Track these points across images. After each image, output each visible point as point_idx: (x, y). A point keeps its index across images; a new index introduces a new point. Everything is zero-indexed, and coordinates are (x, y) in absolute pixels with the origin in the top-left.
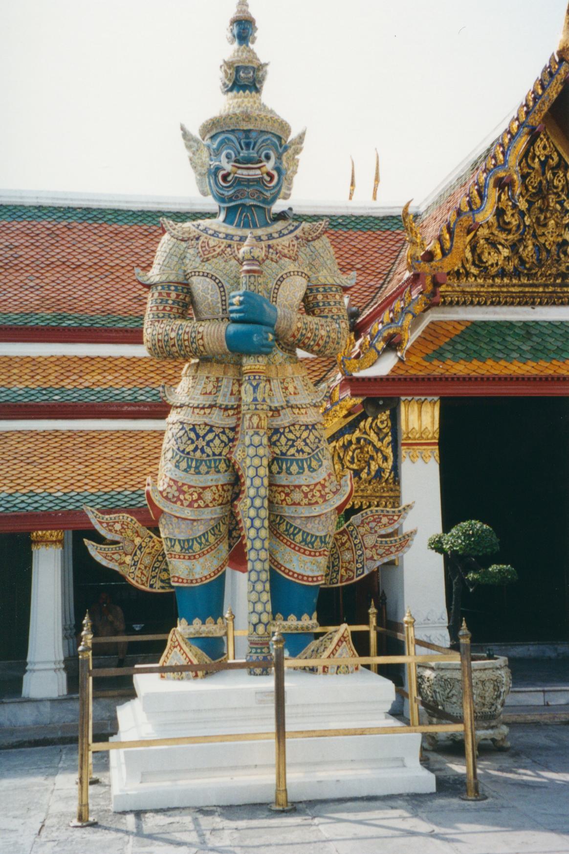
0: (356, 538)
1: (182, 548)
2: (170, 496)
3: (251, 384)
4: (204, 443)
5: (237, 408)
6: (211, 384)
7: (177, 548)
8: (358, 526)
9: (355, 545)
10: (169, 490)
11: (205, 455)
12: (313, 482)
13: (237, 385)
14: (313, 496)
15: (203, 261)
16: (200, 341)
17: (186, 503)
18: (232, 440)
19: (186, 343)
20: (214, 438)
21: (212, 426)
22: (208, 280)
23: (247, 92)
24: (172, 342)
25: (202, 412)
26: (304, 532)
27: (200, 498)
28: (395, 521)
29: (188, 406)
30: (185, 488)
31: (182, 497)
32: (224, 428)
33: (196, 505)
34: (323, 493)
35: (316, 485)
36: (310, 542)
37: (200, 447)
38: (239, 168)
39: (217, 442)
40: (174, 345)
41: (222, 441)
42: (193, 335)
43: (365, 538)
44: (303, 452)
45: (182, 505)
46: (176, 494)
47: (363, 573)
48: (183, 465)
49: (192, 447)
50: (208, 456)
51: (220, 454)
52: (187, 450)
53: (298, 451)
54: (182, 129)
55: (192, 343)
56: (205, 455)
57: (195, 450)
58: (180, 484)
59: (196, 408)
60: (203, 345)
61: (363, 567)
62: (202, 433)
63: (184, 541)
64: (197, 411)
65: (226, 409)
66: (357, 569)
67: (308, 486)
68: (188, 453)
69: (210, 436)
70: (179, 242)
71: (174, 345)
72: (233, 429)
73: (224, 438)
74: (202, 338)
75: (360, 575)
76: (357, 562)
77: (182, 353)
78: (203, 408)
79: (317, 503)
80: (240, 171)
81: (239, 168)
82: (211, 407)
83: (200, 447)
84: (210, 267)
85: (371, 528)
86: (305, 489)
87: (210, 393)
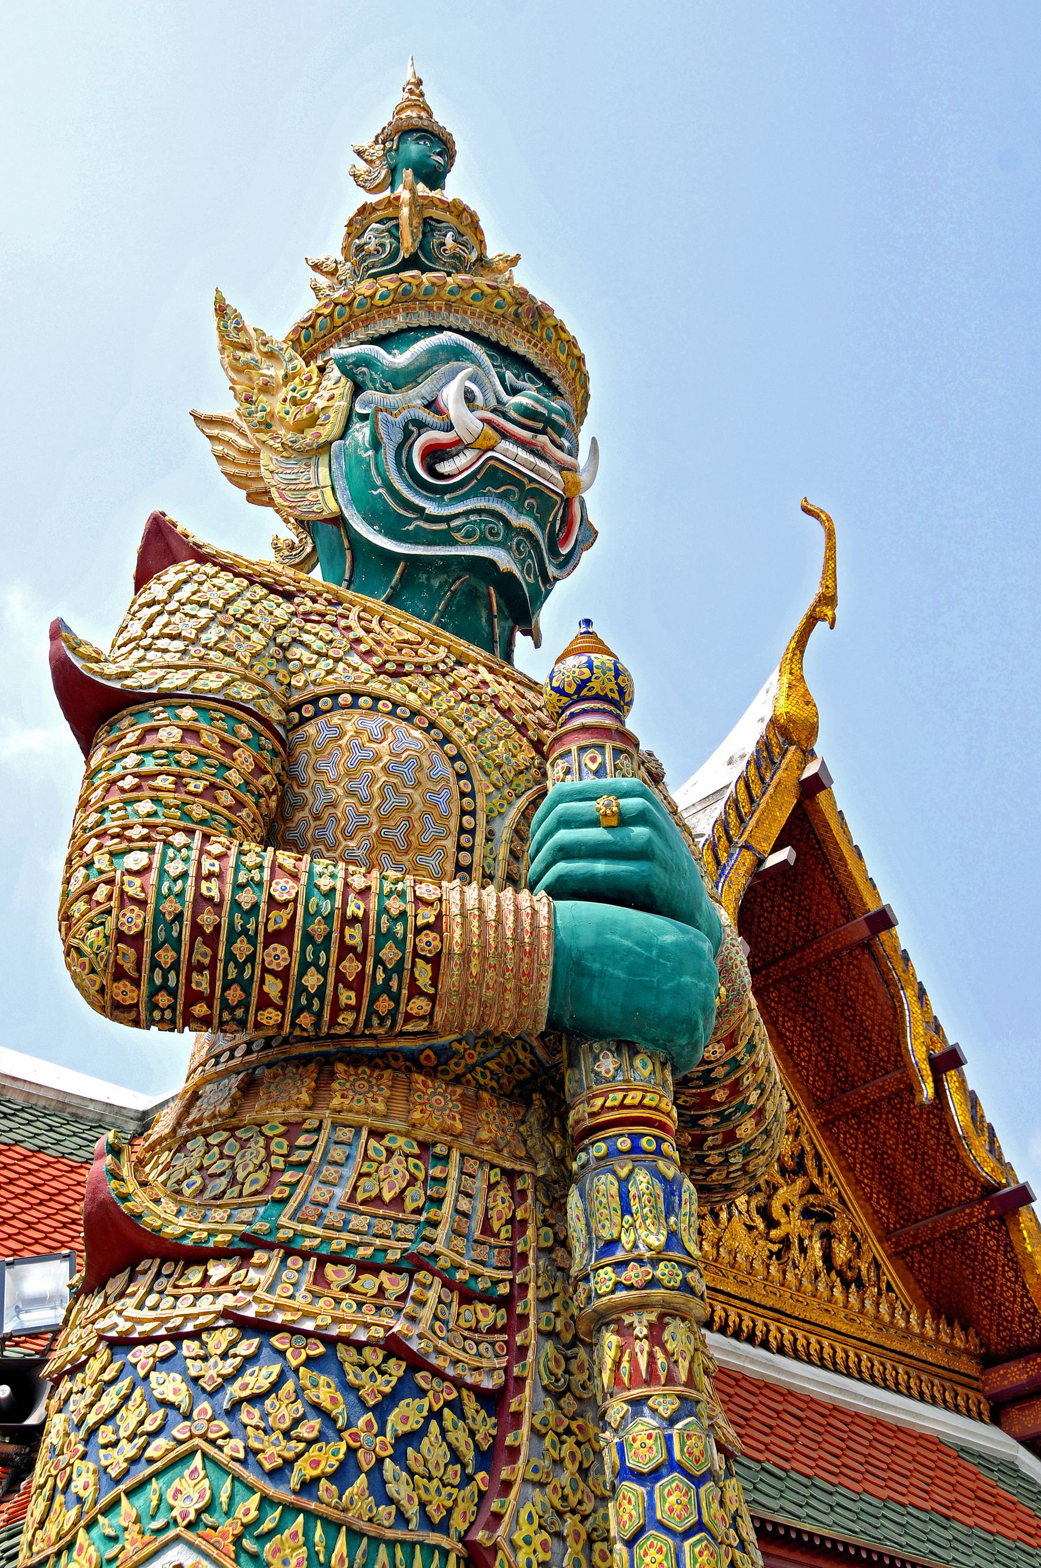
3: (656, 1173)
13: (502, 1192)
19: (354, 935)
20: (427, 1420)
21: (416, 1363)
24: (280, 919)
25: (368, 1283)
29: (289, 1250)
32: (458, 1383)
37: (366, 1460)
38: (505, 435)
39: (432, 1449)
40: (283, 936)
42: (395, 905)
49: (329, 1457)
50: (402, 1519)
52: (303, 1470)
54: (221, 310)
55: (383, 938)
57: (341, 1476)
59: (337, 1259)
62: (375, 1387)
64: (338, 1275)
65: (467, 1297)
68: (309, 1486)
69: (407, 1415)
71: (283, 936)
72: (493, 1401)
73: (460, 1437)
74: (436, 926)
77: (312, 980)
78: (366, 1267)
81: (505, 435)
82: (413, 1264)
83: (366, 1460)
87: (399, 1199)
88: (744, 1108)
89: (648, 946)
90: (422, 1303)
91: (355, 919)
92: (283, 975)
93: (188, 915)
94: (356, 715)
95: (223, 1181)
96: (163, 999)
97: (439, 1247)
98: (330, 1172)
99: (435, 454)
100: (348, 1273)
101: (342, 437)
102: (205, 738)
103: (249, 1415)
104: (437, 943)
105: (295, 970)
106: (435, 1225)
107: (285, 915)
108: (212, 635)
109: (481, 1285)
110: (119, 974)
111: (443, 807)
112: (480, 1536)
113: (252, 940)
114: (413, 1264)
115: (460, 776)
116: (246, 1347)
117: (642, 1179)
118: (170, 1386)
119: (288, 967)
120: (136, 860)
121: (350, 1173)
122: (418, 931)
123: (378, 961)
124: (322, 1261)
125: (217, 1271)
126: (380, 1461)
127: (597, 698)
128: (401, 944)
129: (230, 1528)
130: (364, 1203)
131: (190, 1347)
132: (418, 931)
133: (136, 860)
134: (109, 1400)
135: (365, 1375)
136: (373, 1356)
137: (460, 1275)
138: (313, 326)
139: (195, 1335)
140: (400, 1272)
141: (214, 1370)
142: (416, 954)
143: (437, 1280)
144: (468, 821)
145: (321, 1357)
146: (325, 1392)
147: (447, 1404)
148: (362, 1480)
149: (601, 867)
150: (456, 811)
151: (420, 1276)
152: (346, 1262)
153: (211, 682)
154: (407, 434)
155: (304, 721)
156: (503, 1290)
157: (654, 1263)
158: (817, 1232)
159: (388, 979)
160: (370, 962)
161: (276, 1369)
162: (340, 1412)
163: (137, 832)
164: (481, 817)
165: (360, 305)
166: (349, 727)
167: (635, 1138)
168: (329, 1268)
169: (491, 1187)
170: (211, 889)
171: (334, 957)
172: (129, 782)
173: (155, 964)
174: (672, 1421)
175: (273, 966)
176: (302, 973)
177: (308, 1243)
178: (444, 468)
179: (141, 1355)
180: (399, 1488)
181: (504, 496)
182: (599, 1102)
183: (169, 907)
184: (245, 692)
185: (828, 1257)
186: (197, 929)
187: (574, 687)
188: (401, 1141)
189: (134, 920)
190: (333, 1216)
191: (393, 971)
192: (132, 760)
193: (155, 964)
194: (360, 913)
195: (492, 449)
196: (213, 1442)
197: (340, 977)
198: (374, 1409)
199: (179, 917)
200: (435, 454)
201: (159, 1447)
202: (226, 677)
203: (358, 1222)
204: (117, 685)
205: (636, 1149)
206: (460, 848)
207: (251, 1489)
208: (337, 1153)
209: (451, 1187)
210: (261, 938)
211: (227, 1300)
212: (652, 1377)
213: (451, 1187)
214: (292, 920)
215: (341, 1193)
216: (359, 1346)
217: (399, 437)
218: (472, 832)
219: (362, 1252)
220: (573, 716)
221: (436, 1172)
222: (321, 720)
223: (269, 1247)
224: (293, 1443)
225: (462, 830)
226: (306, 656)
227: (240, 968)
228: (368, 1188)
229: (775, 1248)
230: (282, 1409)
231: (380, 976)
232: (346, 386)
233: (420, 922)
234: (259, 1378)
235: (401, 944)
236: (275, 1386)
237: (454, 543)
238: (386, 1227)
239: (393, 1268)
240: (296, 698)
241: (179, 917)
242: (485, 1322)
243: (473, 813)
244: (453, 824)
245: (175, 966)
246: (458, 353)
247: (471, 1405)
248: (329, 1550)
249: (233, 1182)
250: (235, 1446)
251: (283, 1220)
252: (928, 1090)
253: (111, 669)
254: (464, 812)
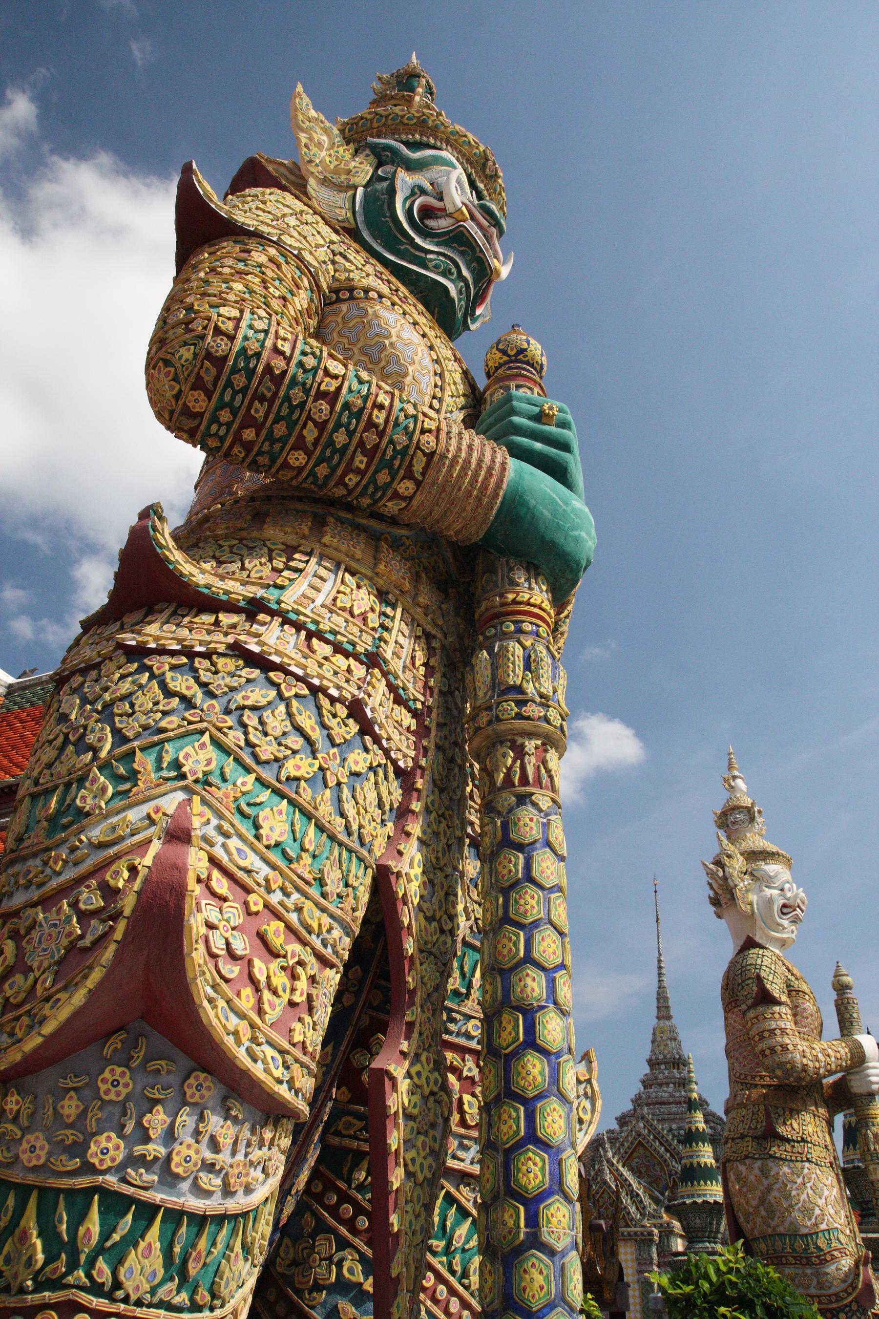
19: (380, 417)
31: (260, 969)
38: (473, 218)
71: (332, 397)
77: (340, 438)
81: (473, 218)
92: (321, 426)
96: (225, 416)
100: (327, 650)
104: (433, 444)
105: (331, 426)
110: (199, 384)
113: (307, 392)
119: (326, 422)
125: (226, 619)
132: (423, 431)
136: (342, 711)
138: (357, 124)
145: (304, 697)
149: (538, 446)
154: (413, 193)
155: (339, 300)
159: (393, 458)
160: (385, 440)
165: (393, 119)
171: (362, 425)
173: (229, 384)
175: (316, 417)
176: (336, 429)
178: (432, 223)
181: (462, 254)
187: (515, 351)
191: (399, 452)
193: (229, 384)
196: (220, 730)
197: (361, 443)
199: (258, 355)
210: (313, 392)
217: (408, 193)
220: (510, 368)
224: (282, 748)
227: (292, 408)
231: (389, 453)
235: (410, 435)
237: (426, 268)
245: (244, 390)
254: (434, 397)
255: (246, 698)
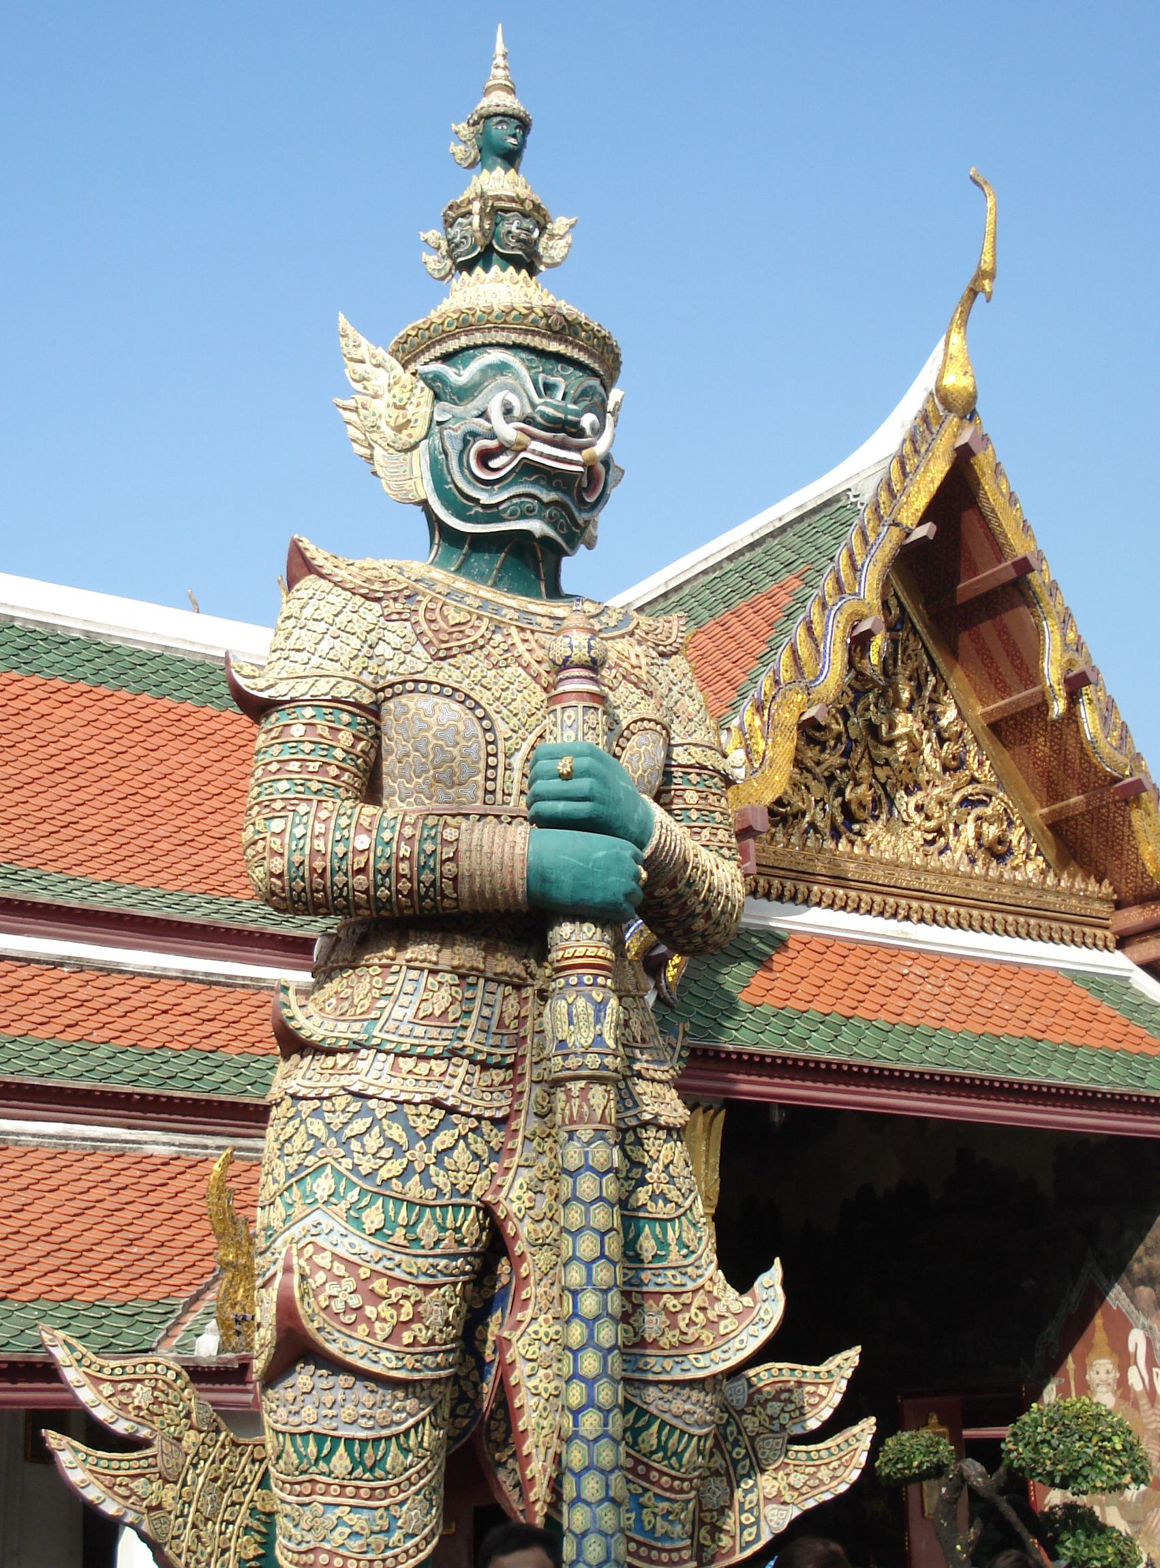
0: (736, 1443)
1: (356, 1463)
2: (338, 1306)
3: (590, 998)
4: (430, 1158)
5: (511, 1066)
6: (444, 992)
7: (341, 1461)
8: (741, 1412)
9: (735, 1462)
10: (331, 1289)
11: (430, 1193)
12: (691, 1286)
13: (513, 1000)
14: (691, 1323)
15: (435, 658)
16: (450, 866)
17: (382, 1330)
18: (496, 1154)
19: (404, 867)
20: (457, 1141)
21: (451, 1110)
22: (456, 707)
23: (524, 272)
24: (360, 861)
25: (423, 1067)
26: (663, 1424)
27: (417, 1317)
28: (822, 1398)
30: (379, 1285)
31: (370, 1311)
32: (479, 1118)
33: (407, 1337)
34: (712, 1315)
35: (695, 1291)
36: (675, 1453)
39: (461, 1155)
41: (476, 1156)
42: (429, 847)
43: (758, 1443)
44: (667, 1201)
45: (371, 1334)
46: (355, 1301)
47: (758, 1537)
48: (373, 1218)
49: (396, 1167)
51: (467, 1194)
52: (384, 1174)
53: (653, 1197)
56: (430, 1193)
57: (404, 1175)
58: (364, 1273)
59: (404, 1054)
60: (455, 879)
61: (757, 1523)
62: (423, 1126)
63: (364, 1442)
64: (406, 1064)
65: (485, 1066)
66: (743, 1527)
67: (676, 1295)
69: (444, 1139)
70: (358, 600)
73: (480, 1147)
75: (749, 1544)
76: (742, 1511)
78: (421, 1057)
79: (698, 1341)
80: (535, 445)
81: (533, 437)
83: (419, 1167)
84: (456, 674)
85: (771, 1418)
86: (671, 1302)
87: (445, 1012)
88: (693, 915)
89: (586, 861)
90: (454, 1077)
91: (404, 858)
92: (366, 892)
93: (307, 863)
94: (416, 696)
95: (346, 1004)
97: (466, 1042)
98: (404, 1000)
99: (485, 457)
101: (426, 437)
102: (319, 730)
103: (355, 1145)
104: (455, 869)
106: (465, 1028)
107: (363, 859)
108: (324, 648)
109: (494, 1060)
111: (474, 756)
112: (489, 1198)
113: (346, 874)
114: (452, 1053)
115: (486, 730)
116: (355, 1106)
117: (581, 1002)
118: (317, 1127)
120: (277, 825)
121: (416, 1000)
122: (443, 862)
123: (420, 882)
124: (397, 1055)
125: (342, 1059)
126: (427, 1165)
127: (577, 666)
128: (433, 870)
129: (344, 1205)
130: (423, 1018)
131: (327, 1105)
132: (443, 862)
133: (277, 825)
134: (289, 1130)
135: (419, 1121)
137: (480, 1057)
139: (329, 1098)
140: (442, 1059)
141: (337, 1120)
142: (442, 876)
143: (466, 1061)
144: (492, 761)
146: (396, 1132)
147: (471, 1130)
148: (417, 1177)
150: (483, 755)
151: (454, 1060)
152: (410, 1056)
153: (322, 687)
154: (466, 443)
156: (509, 1060)
157: (584, 1054)
158: (971, 818)
161: (369, 1120)
162: (403, 1141)
163: (278, 805)
164: (501, 756)
165: (435, 330)
166: (411, 705)
167: (580, 976)
168: (401, 1059)
169: (505, 997)
170: (319, 844)
172: (274, 767)
174: (589, 1143)
177: (388, 1046)
178: (494, 464)
179: (306, 1107)
180: (440, 1179)
181: (535, 483)
182: (560, 954)
183: (297, 858)
184: (345, 690)
185: (978, 837)
186: (313, 870)
188: (448, 977)
189: (278, 865)
190: (405, 1029)
192: (275, 750)
194: (408, 855)
195: (524, 450)
196: (336, 1159)
197: (398, 892)
198: (424, 1139)
200: (485, 457)
201: (310, 1160)
202: (333, 681)
203: (420, 1031)
204: (265, 695)
205: (580, 983)
206: (487, 779)
207: (355, 1185)
208: (409, 987)
209: (478, 1002)
210: (350, 873)
211: (345, 1081)
212: (581, 1119)
213: (478, 1002)
214: (367, 863)
215: (411, 1012)
216: (416, 1105)
217: (459, 446)
218: (495, 767)
219: (419, 1050)
221: (468, 994)
222: (395, 700)
223: (369, 1048)
225: (488, 767)
226: (389, 653)
228: (426, 1008)
229: (930, 837)
230: (372, 1142)
232: (428, 394)
233: (444, 857)
234: (359, 1125)
235: (433, 870)
236: (369, 1129)
237: (502, 520)
238: (434, 1032)
239: (436, 1057)
240: (382, 683)
241: (302, 863)
242: (497, 1080)
243: (495, 755)
244: (482, 765)
246: (502, 368)
247: (486, 1127)
248: (397, 1214)
249: (352, 1005)
250: (347, 1163)
251: (376, 1033)
252: (1059, 707)
253: (262, 683)
254: (489, 755)
255: (351, 1130)
